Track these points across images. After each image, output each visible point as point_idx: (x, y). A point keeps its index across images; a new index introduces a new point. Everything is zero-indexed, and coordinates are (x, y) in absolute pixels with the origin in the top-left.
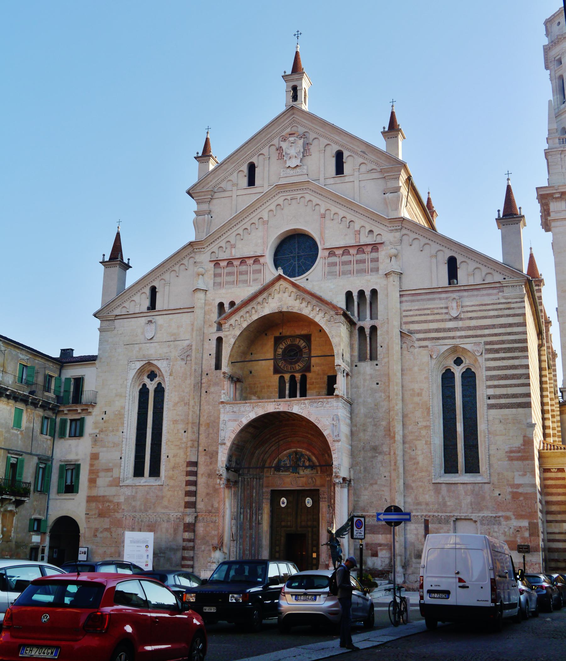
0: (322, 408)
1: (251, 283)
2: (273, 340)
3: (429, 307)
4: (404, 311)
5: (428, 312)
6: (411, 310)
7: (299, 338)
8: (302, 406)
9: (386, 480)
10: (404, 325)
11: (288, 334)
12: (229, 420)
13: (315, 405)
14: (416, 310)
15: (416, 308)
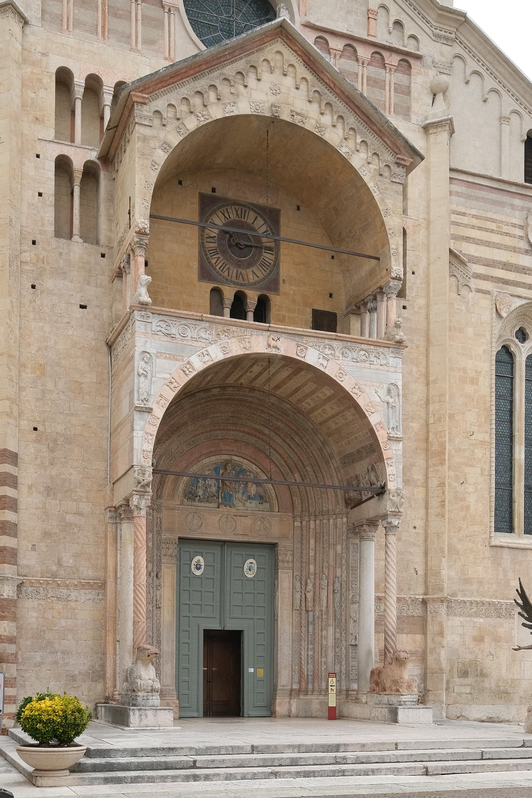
0: (367, 365)
1: (140, 45)
2: (196, 200)
3: (494, 216)
4: (454, 212)
5: (493, 226)
6: (464, 214)
7: (255, 211)
8: (327, 351)
9: (417, 534)
10: (452, 241)
11: (230, 195)
12: (159, 355)
13: (355, 355)
14: (473, 216)
15: (474, 212)
